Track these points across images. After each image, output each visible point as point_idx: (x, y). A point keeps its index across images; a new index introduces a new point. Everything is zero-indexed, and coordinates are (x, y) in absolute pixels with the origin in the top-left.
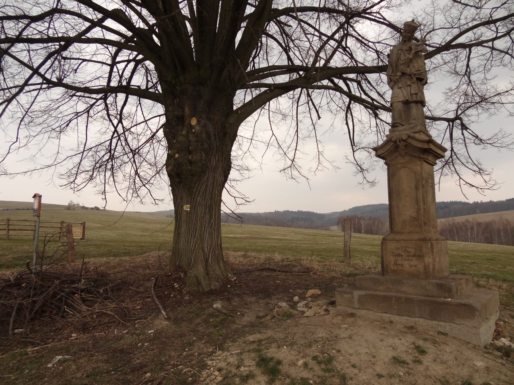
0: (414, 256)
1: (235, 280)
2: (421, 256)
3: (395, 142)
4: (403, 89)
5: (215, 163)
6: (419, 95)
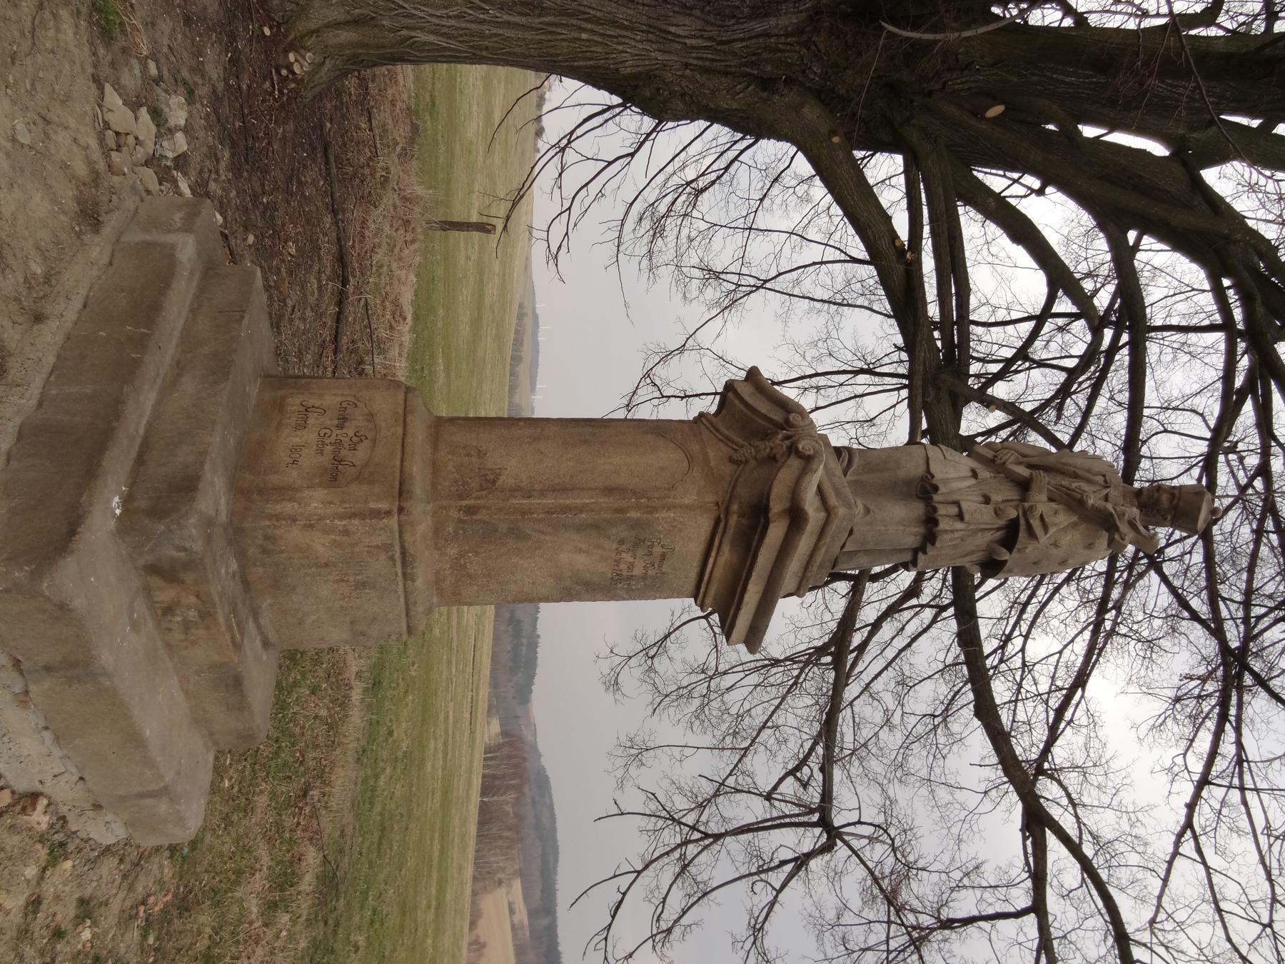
0: (338, 460)
1: (289, 67)
2: (334, 478)
3: (787, 424)
4: (973, 481)
5: (680, 31)
6: (959, 525)
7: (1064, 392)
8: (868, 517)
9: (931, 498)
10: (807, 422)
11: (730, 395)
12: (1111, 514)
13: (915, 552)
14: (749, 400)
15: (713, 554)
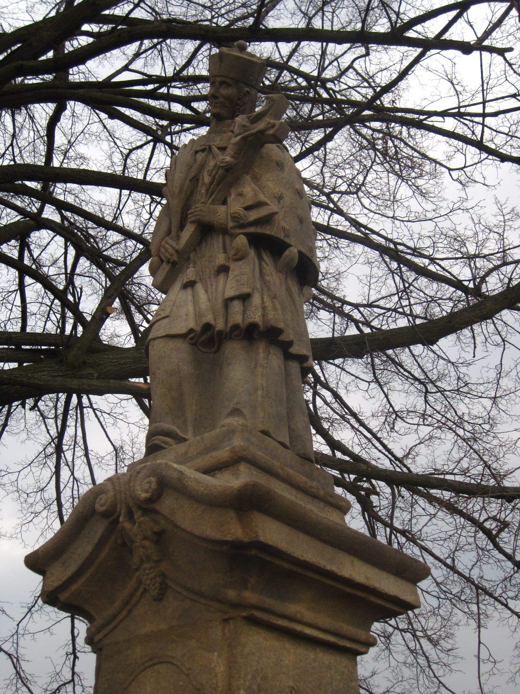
3: (110, 515)
4: (199, 287)
6: (256, 300)
7: (98, 258)
8: (246, 411)
9: (220, 332)
10: (110, 487)
11: (63, 597)
12: (244, 138)
13: (288, 356)
14: (69, 572)
15: (299, 628)
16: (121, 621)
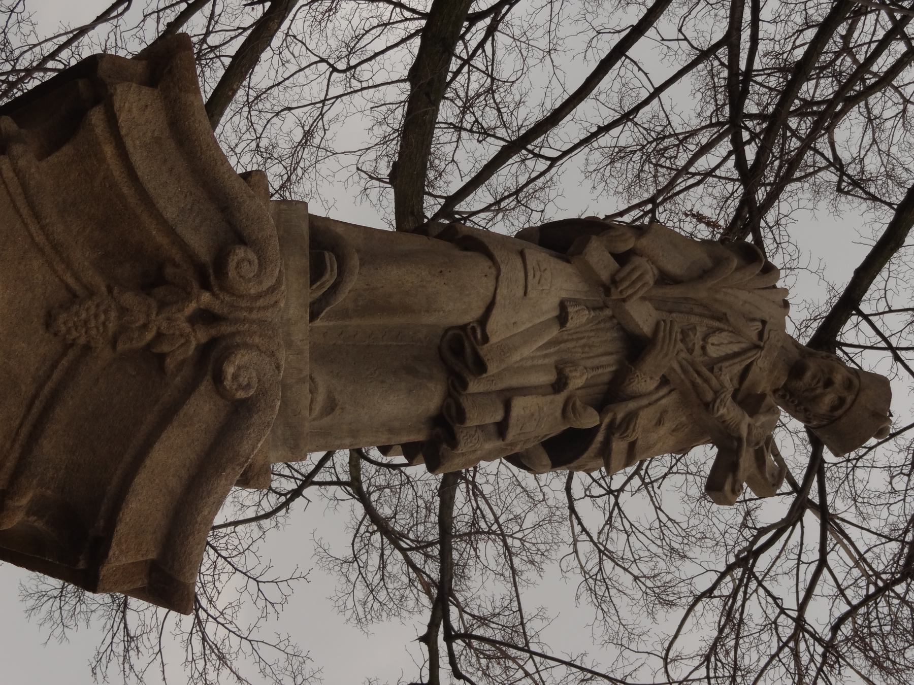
8: (327, 420)
9: (465, 386)
12: (740, 439)
14: (138, 158)
16: (26, 225)
